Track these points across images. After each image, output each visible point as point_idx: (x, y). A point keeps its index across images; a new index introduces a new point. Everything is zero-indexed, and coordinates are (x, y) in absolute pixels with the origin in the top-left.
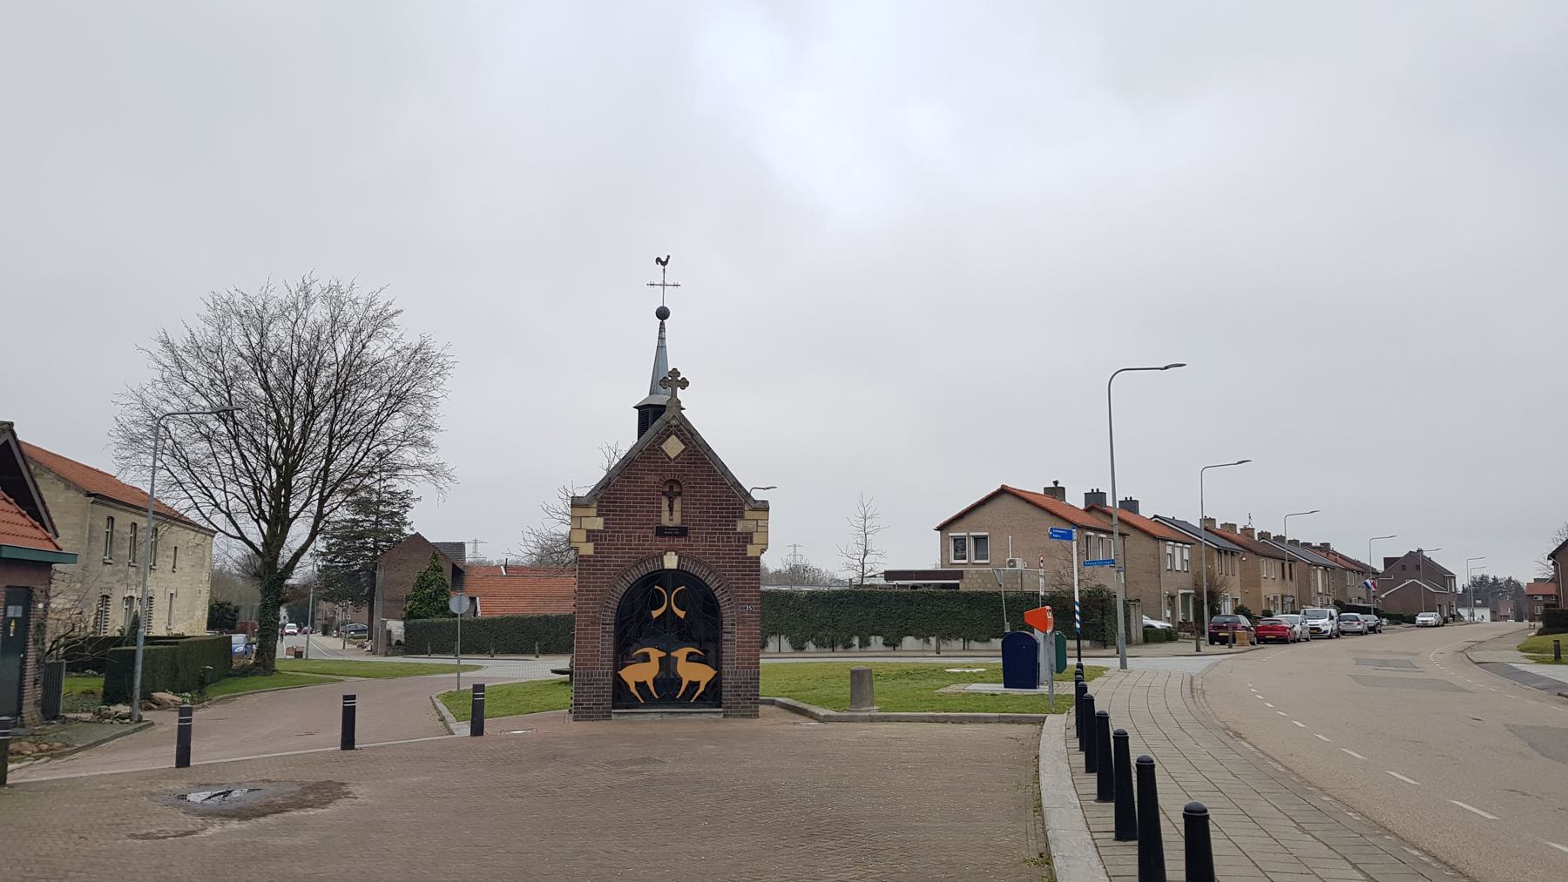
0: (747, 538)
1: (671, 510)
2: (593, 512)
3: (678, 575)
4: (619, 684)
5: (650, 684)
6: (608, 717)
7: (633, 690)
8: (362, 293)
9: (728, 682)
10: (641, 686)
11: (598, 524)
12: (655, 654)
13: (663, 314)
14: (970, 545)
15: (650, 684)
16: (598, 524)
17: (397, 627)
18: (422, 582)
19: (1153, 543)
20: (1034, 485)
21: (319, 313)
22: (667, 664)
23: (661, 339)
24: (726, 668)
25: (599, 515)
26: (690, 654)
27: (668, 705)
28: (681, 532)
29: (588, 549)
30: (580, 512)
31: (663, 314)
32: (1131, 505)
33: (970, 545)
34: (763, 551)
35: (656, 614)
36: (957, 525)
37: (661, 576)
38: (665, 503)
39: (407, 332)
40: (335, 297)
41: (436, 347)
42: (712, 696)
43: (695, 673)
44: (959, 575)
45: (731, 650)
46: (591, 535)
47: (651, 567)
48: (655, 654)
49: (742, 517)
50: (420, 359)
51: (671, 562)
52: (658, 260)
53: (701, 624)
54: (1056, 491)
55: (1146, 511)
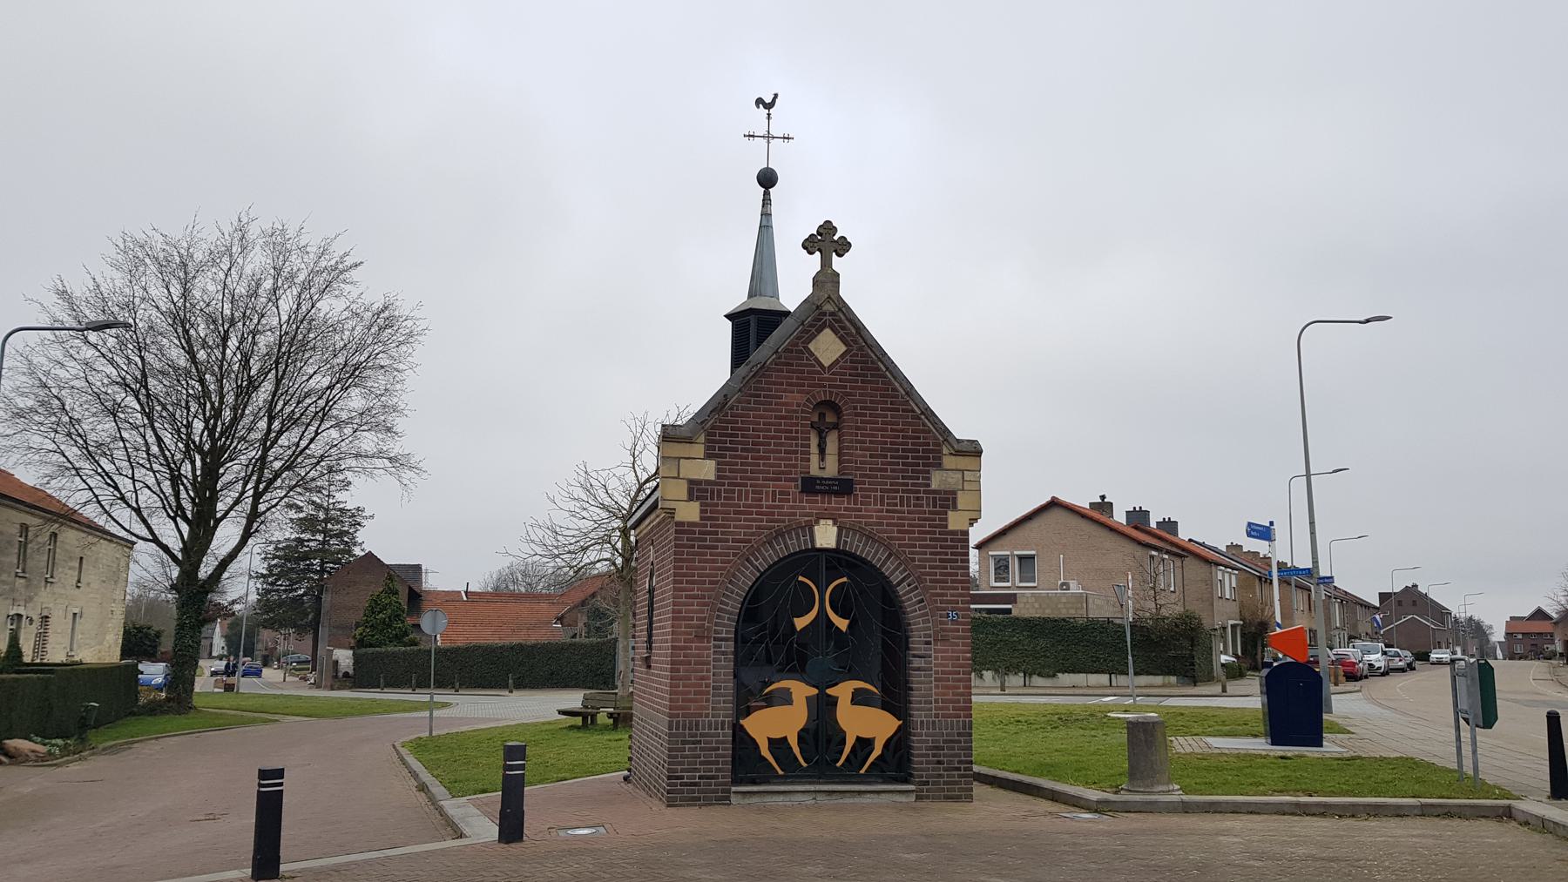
0: (947, 500)
1: (822, 451)
2: (699, 450)
3: (837, 560)
4: (742, 740)
5: (793, 742)
6: (724, 799)
7: (765, 752)
8: (313, 240)
9: (921, 742)
10: (778, 745)
11: (707, 470)
12: (801, 691)
13: (767, 179)
14: (1014, 566)
15: (793, 742)
16: (707, 470)
17: (344, 657)
18: (375, 606)
19: (1205, 567)
20: (1083, 499)
21: (257, 260)
22: (823, 708)
23: (766, 214)
24: (918, 716)
25: (708, 456)
28: (842, 487)
29: (690, 512)
30: (677, 450)
31: (767, 179)
32: (1170, 526)
33: (1014, 566)
34: (973, 521)
35: (800, 623)
36: (992, 545)
39: (368, 288)
40: (279, 246)
41: (403, 309)
42: (895, 764)
43: (866, 723)
44: (1012, 599)
45: (925, 688)
46: (696, 490)
47: (793, 544)
49: (939, 466)
50: (384, 322)
51: (826, 536)
52: (759, 102)
53: (874, 635)
54: (1104, 506)
55: (1184, 534)
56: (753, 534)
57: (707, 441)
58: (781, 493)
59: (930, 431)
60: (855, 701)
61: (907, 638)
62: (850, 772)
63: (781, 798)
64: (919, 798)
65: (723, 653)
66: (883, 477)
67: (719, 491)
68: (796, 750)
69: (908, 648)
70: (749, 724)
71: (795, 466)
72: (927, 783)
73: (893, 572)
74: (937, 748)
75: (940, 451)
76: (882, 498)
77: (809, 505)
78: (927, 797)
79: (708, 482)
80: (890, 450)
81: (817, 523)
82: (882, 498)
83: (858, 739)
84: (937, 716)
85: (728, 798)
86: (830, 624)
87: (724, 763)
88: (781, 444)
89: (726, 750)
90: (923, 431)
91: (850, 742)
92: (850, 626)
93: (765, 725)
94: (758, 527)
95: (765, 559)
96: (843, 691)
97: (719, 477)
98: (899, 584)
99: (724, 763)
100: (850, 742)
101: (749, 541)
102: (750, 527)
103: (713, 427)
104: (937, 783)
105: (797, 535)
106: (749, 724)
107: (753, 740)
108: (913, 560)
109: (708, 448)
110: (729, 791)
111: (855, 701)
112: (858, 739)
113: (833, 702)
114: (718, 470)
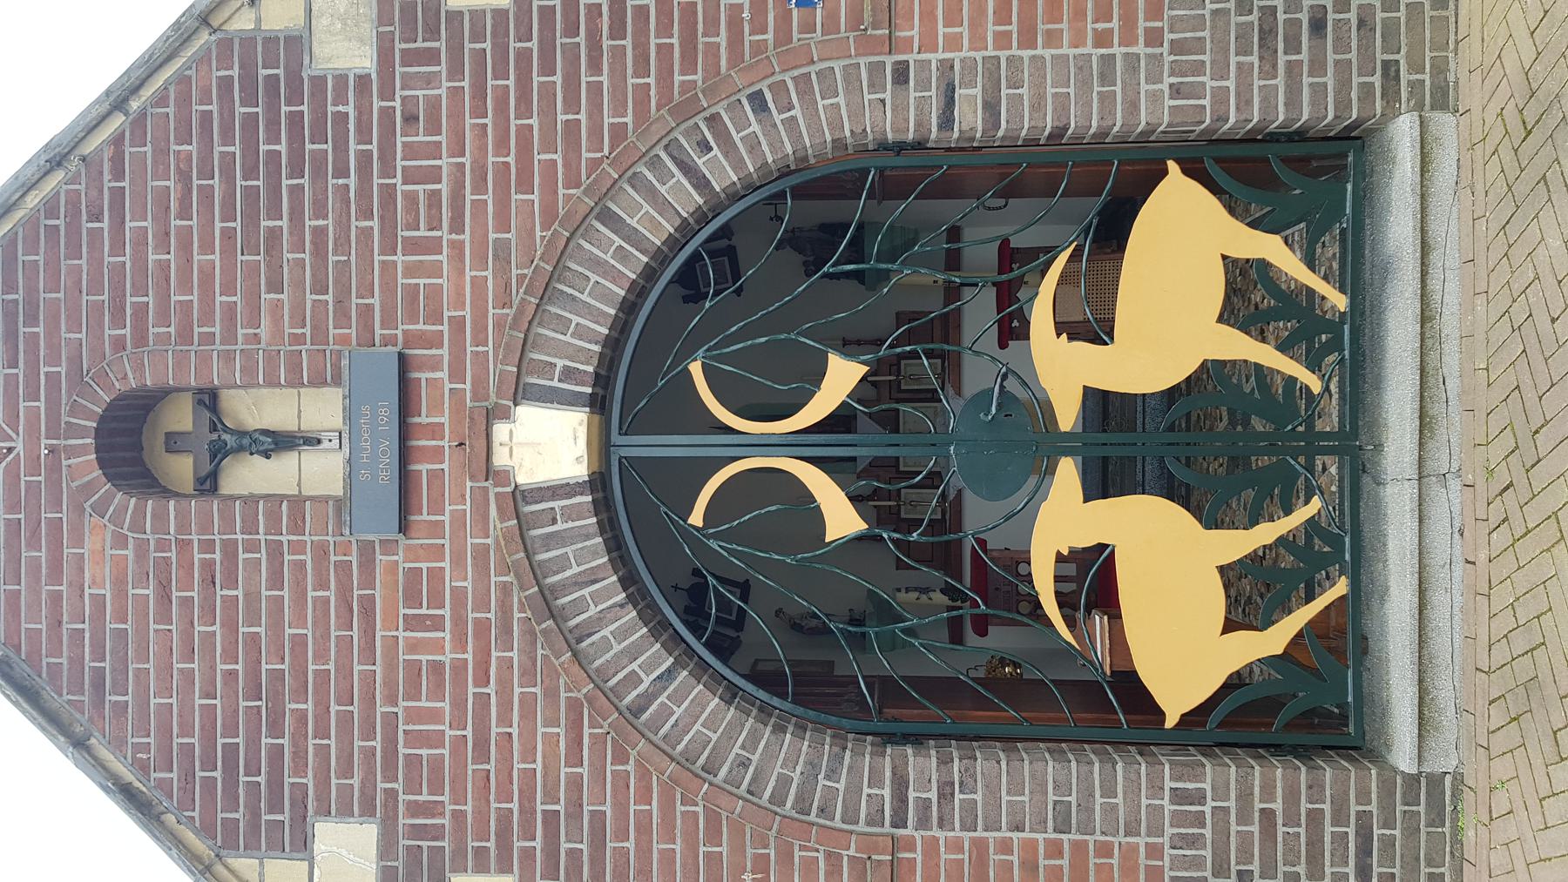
1: (280, 442)
3: (629, 390)
4: (1244, 719)
5: (1238, 543)
6: (1434, 794)
15: (1238, 543)
25: (303, 844)
26: (1069, 329)
27: (1355, 447)
35: (842, 518)
37: (629, 499)
38: (251, 476)
47: (580, 552)
48: (1064, 518)
51: (549, 444)
56: (551, 694)
57: (252, 847)
58: (413, 598)
59: (183, 80)
61: (883, 146)
62: (1348, 344)
63: (1440, 600)
64: (1442, 99)
65: (946, 794)
66: (342, 244)
67: (415, 809)
68: (1265, 534)
69: (919, 145)
71: (321, 552)
72: (1390, 72)
73: (658, 210)
74: (1267, 34)
75: (248, 41)
76: (413, 246)
77: (450, 502)
78: (1440, 69)
79: (387, 846)
80: (251, 219)
81: (503, 476)
82: (413, 246)
84: (1154, 38)
85: (1436, 781)
86: (840, 421)
87: (1315, 788)
88: (252, 597)
89: (1273, 781)
90: (184, 101)
91: (1238, 346)
92: (849, 346)
93: (1183, 646)
94: (528, 675)
95: (632, 654)
96: (1063, 372)
97: (368, 811)
98: (701, 183)
99: (1315, 788)
100: (1238, 346)
101: (575, 706)
102: (528, 703)
103: (207, 830)
104: (1391, 30)
105: (550, 541)
107: (1234, 683)
108: (618, 132)
109: (277, 847)
110: (1412, 781)
113: (1102, 406)
114: (345, 812)
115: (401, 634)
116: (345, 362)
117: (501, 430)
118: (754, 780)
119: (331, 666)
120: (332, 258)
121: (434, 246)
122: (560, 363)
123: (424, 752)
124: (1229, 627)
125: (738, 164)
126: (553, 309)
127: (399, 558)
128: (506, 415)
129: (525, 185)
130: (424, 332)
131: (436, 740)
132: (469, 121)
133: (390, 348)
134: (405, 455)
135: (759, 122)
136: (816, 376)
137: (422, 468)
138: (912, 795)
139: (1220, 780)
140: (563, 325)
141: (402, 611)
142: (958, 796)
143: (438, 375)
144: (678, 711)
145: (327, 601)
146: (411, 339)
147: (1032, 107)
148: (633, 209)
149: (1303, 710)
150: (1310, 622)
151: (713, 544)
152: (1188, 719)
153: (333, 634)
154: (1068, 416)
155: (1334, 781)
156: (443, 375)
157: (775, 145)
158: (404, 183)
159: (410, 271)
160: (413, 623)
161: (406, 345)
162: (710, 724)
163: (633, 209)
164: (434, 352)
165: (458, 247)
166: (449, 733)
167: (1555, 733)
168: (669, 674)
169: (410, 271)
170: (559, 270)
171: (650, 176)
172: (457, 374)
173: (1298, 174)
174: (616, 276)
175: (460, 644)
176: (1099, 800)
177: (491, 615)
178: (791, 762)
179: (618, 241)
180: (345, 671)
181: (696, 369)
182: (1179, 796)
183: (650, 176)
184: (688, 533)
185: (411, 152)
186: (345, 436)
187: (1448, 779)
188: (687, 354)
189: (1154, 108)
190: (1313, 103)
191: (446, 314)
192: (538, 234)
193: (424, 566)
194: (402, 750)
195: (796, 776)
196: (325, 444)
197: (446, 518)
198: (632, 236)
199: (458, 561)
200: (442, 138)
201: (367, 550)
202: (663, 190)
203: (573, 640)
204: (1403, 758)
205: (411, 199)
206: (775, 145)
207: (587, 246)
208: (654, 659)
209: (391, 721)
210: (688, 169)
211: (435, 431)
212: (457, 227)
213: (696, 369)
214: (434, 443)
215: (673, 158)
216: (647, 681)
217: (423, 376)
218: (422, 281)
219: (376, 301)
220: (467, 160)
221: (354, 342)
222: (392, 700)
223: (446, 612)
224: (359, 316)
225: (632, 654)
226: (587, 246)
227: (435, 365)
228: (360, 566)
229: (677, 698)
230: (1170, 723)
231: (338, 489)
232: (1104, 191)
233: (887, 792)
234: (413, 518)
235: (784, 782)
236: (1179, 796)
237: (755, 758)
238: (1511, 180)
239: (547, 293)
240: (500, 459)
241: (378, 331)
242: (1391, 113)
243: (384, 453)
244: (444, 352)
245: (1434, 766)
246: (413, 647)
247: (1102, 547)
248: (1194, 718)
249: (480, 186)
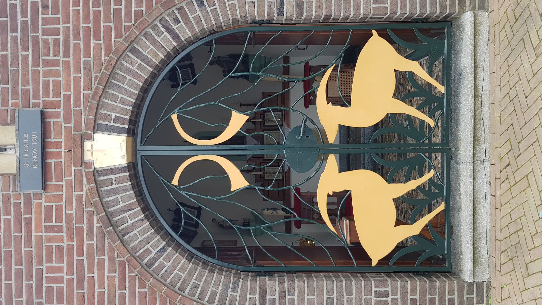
3: (145, 126)
7: (415, 229)
26: (332, 100)
27: (448, 149)
35: (238, 181)
37: (145, 174)
47: (123, 198)
48: (331, 179)
51: (109, 150)
56: (111, 259)
58: (49, 218)
60: (343, 101)
61: (254, 22)
62: (444, 106)
63: (481, 211)
66: (15, 62)
68: (412, 185)
69: (270, 22)
70: (377, 251)
73: (157, 48)
76: (47, 63)
77: (65, 176)
81: (89, 165)
82: (47, 63)
83: (397, 95)
85: (480, 285)
87: (432, 289)
89: (415, 287)
92: (241, 107)
93: (379, 230)
94: (101, 251)
95: (147, 241)
96: (331, 119)
98: (176, 37)
99: (432, 289)
101: (122, 264)
102: (101, 263)
105: (110, 193)
106: (377, 251)
107: (400, 247)
108: (139, 14)
111: (343, 101)
112: (397, 95)
115: (44, 234)
116: (16, 115)
117: (87, 144)
118: (201, 293)
119: (12, 249)
120: (10, 68)
121: (56, 63)
122: (114, 115)
123: (55, 286)
124: (398, 223)
125: (192, 29)
126: (111, 91)
127: (42, 201)
128: (90, 138)
129: (97, 36)
130: (52, 101)
131: (60, 280)
132: (72, 8)
133: (37, 108)
134: (44, 156)
135: (201, 10)
136: (227, 120)
137: (52, 161)
138: (268, 297)
139: (394, 287)
140: (115, 98)
141: (44, 224)
142: (287, 297)
143: (59, 120)
144: (168, 265)
145: (10, 220)
146: (46, 104)
147: (316, 6)
148: (146, 48)
149: (426, 256)
150: (430, 221)
151: (183, 193)
152: (380, 262)
153: (13, 235)
154: (332, 137)
155: (440, 286)
156: (61, 120)
157: (208, 20)
158: (43, 35)
159: (46, 74)
160: (49, 229)
161: (44, 107)
162: (182, 270)
163: (146, 48)
164: (57, 110)
165: (67, 64)
166: (66, 277)
167: (526, 265)
168: (164, 249)
169: (46, 74)
170: (113, 74)
171: (153, 33)
172: (67, 119)
173: (425, 37)
174: (139, 77)
175: (70, 237)
176: (345, 297)
177: (84, 225)
178: (217, 285)
179: (139, 62)
180: (19, 251)
181: (174, 117)
182: (378, 294)
183: (153, 33)
184: (172, 189)
185: (46, 21)
186: (17, 147)
187: (485, 284)
188: (171, 111)
189: (368, 9)
190: (431, 7)
191: (62, 93)
192: (103, 58)
193: (54, 204)
194: (45, 285)
195: (219, 291)
196: (8, 151)
197: (63, 183)
198: (145, 59)
199: (69, 202)
200: (60, 16)
201: (28, 198)
202: (159, 39)
203: (121, 236)
204: (467, 276)
205: (46, 42)
206: (208, 20)
207: (125, 63)
208: (157, 243)
209: (40, 273)
210: (170, 30)
211: (58, 145)
212: (67, 54)
213: (174, 117)
214: (57, 150)
215: (163, 26)
216: (154, 252)
217: (52, 120)
218: (51, 79)
219: (30, 88)
220: (71, 25)
221: (21, 106)
222: (40, 263)
223: (64, 224)
224: (23, 94)
225: (147, 241)
226: (125, 63)
227: (58, 116)
228: (25, 204)
229: (167, 259)
230: (374, 263)
231: (14, 171)
232: (347, 42)
233: (257, 296)
234: (48, 183)
235: (214, 294)
236: (378, 294)
237: (201, 284)
238: (510, 39)
239: (108, 84)
240: (87, 157)
241: (32, 101)
242: (462, 11)
243: (35, 155)
244: (62, 110)
245: (479, 279)
246: (49, 240)
247: (346, 191)
248: (384, 261)
249: (77, 36)
